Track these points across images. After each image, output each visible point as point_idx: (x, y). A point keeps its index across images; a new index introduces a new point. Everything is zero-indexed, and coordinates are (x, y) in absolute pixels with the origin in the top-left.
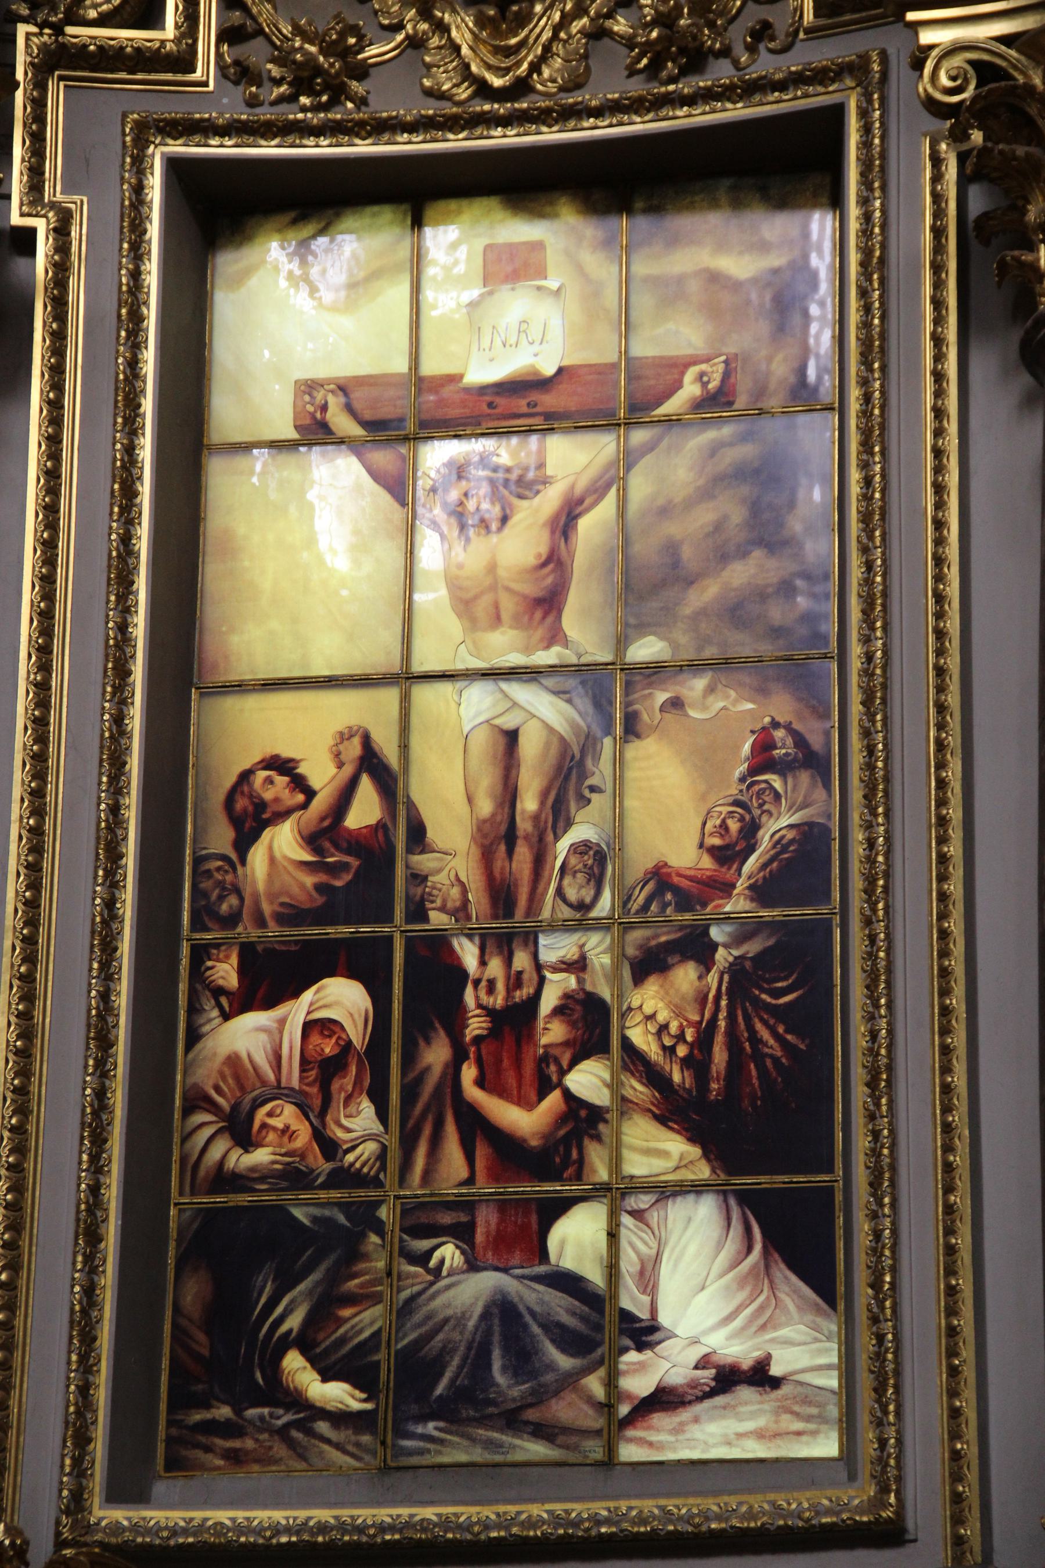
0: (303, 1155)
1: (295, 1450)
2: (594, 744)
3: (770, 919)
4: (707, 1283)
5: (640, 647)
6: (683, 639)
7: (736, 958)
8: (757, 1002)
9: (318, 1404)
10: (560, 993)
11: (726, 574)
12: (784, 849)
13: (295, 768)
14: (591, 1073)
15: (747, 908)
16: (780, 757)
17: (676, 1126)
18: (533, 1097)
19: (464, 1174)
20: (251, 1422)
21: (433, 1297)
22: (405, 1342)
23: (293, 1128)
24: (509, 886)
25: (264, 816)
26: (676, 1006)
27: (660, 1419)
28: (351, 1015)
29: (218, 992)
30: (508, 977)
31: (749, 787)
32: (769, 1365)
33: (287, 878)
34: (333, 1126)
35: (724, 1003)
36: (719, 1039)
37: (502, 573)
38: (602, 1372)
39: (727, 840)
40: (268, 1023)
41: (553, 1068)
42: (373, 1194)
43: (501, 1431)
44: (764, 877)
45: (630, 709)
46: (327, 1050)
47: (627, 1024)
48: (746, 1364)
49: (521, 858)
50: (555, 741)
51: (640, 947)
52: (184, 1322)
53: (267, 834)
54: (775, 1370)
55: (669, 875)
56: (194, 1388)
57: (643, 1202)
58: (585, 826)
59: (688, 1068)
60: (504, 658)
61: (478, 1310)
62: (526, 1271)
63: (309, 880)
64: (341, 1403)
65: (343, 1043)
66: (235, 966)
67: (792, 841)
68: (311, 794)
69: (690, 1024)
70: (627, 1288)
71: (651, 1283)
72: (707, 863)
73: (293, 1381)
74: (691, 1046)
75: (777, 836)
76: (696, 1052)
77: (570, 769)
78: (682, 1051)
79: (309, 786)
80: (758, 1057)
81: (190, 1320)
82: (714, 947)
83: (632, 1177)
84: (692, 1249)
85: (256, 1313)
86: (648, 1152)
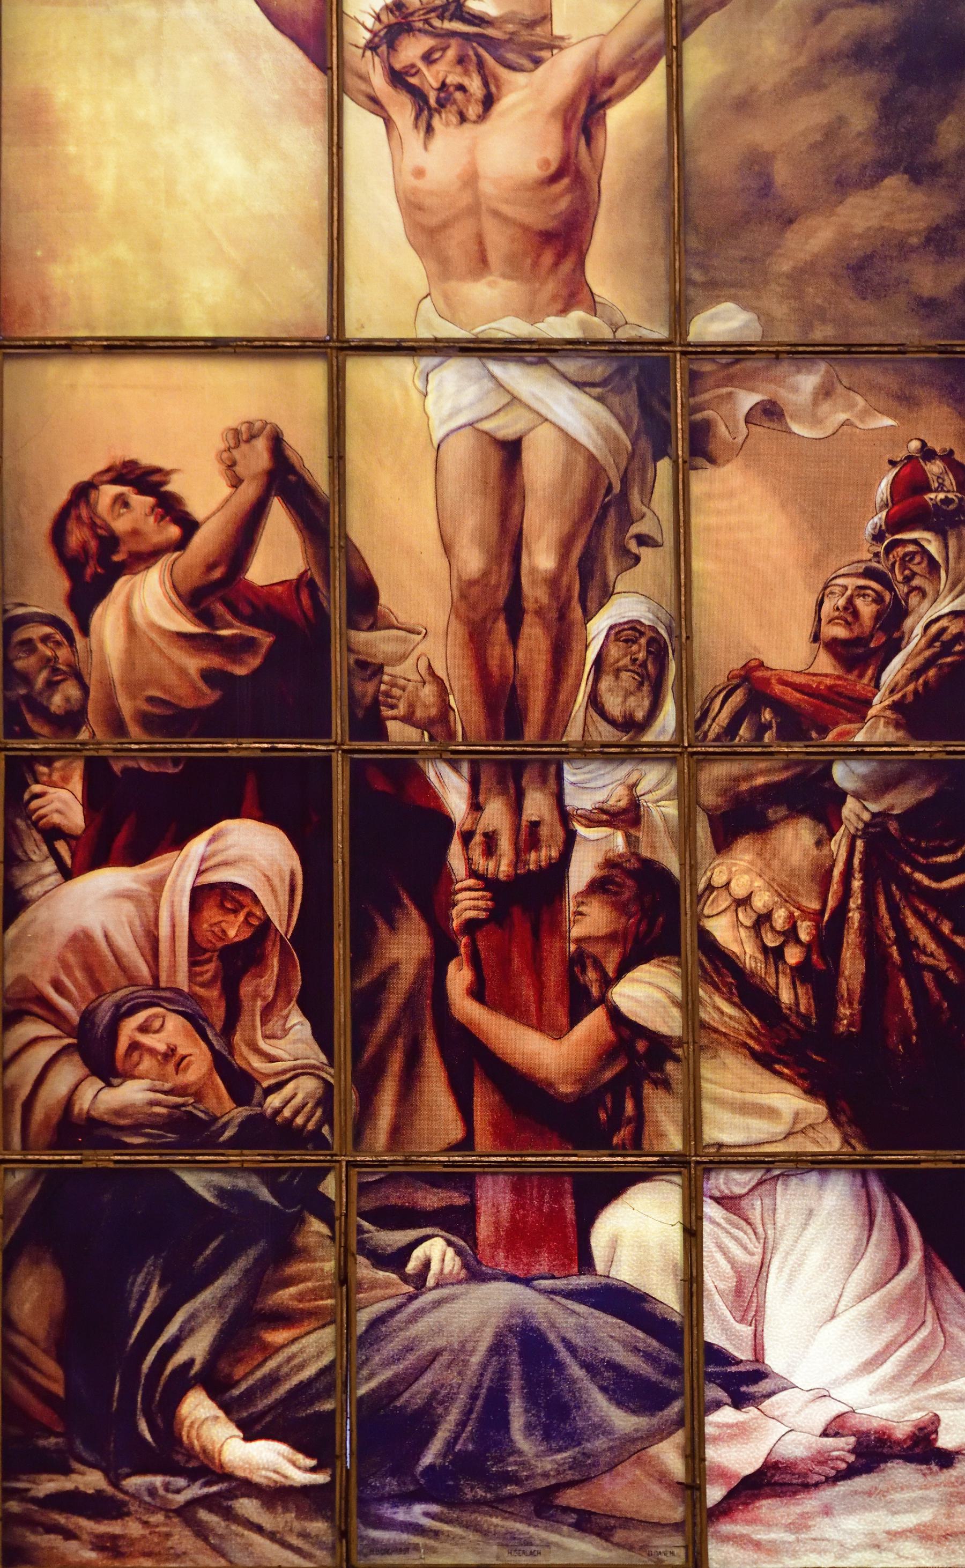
0: (199, 1096)
1: (206, 1540)
2: (643, 470)
3: (926, 757)
4: (841, 1307)
5: (712, 319)
6: (780, 310)
7: (874, 815)
8: (908, 885)
9: (240, 1473)
10: (600, 859)
11: (840, 209)
12: (946, 649)
13: (164, 483)
14: (651, 984)
15: (890, 738)
16: (935, 505)
17: (786, 1071)
18: (562, 1017)
19: (456, 1132)
20: (135, 1496)
21: (413, 1319)
22: (373, 1384)
23: (181, 1051)
24: (514, 687)
25: (116, 558)
26: (781, 885)
27: (767, 1507)
28: (268, 879)
29: (52, 834)
30: (516, 830)
31: (888, 550)
32: (936, 1432)
33: (155, 657)
34: (245, 1050)
35: (857, 884)
36: (851, 938)
37: (486, 187)
38: (679, 1437)
39: (857, 631)
40: (134, 886)
41: (591, 974)
42: (312, 1158)
43: (528, 1520)
44: (916, 692)
45: (698, 416)
46: (232, 933)
47: (707, 911)
48: (901, 1431)
49: (532, 643)
50: (581, 462)
51: (724, 792)
52: (21, 1342)
53: (121, 586)
54: (946, 1440)
55: (767, 681)
56: (42, 1443)
57: (738, 1184)
58: (633, 598)
59: (803, 983)
60: (493, 325)
61: (486, 1341)
62: (559, 1284)
63: (193, 664)
64: (276, 1472)
65: (255, 922)
66: (79, 795)
67: (958, 638)
68: (189, 526)
69: (805, 913)
70: (715, 1313)
71: (754, 1305)
72: (825, 664)
73: (199, 1437)
74: (808, 948)
75: (934, 629)
76: (815, 957)
77: (605, 508)
78: (793, 956)
79: (187, 514)
80: (913, 970)
81: (32, 1341)
82: (840, 796)
83: (720, 1146)
84: (816, 1256)
85: (135, 1333)
86: (745, 1109)
